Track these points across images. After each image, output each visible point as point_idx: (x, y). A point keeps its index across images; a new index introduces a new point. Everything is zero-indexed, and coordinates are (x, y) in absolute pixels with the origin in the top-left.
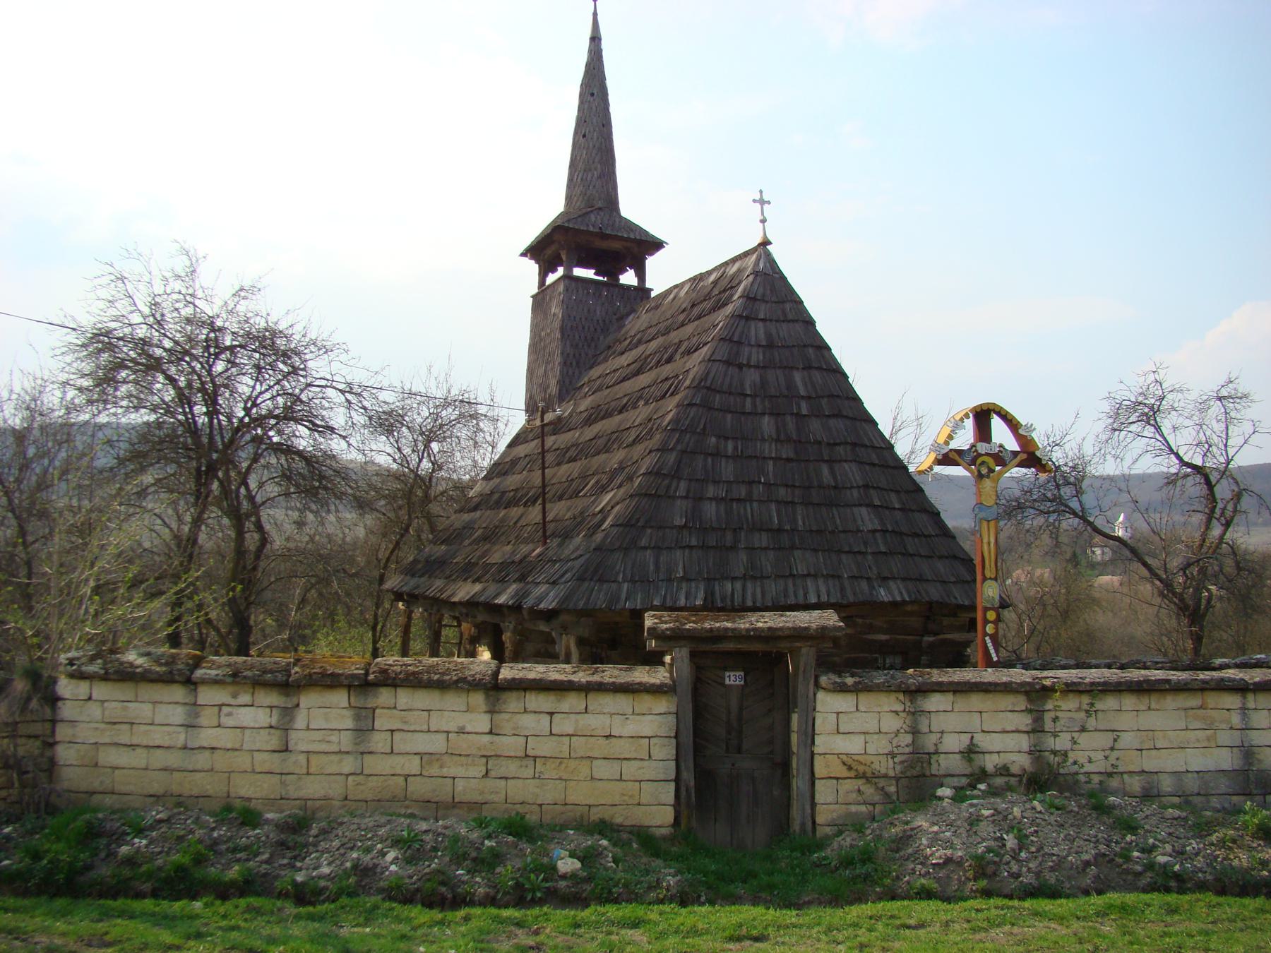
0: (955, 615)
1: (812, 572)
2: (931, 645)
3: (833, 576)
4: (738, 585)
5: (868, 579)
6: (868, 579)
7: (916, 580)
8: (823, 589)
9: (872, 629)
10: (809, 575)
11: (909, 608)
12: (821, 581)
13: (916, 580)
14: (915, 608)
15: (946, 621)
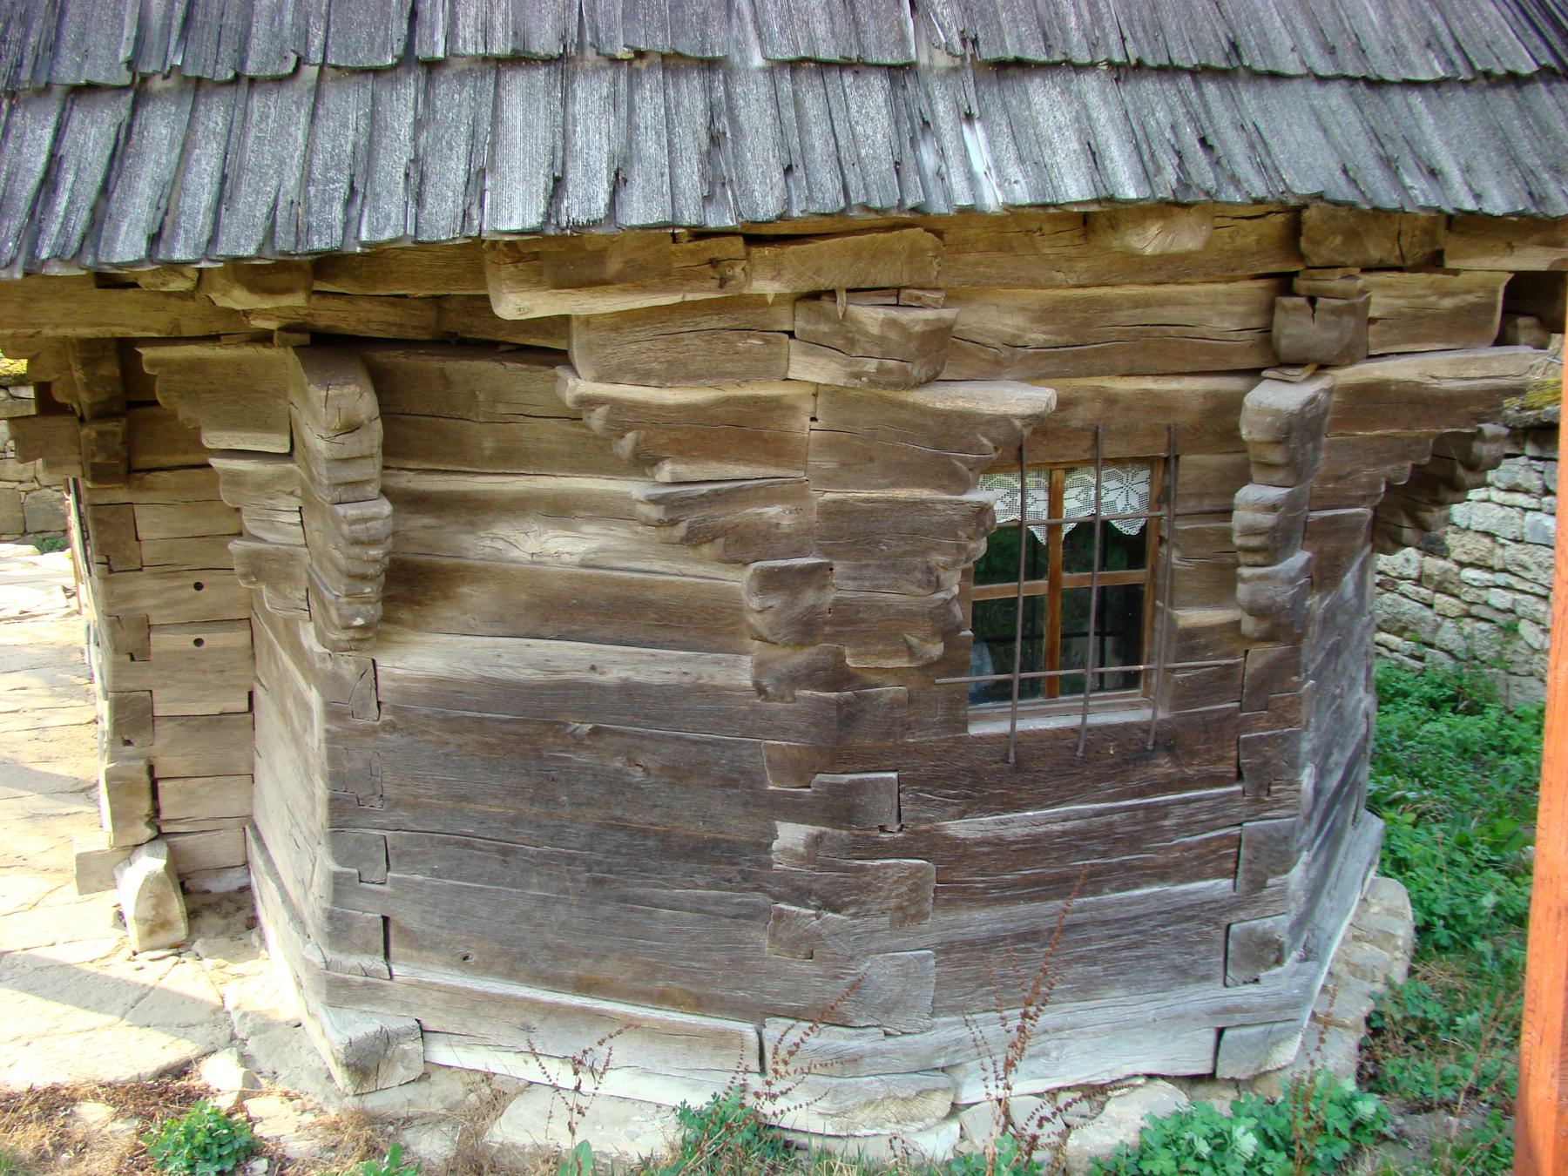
0: (1434, 262)
1: (544, 42)
2: (1298, 431)
3: (673, 63)
4: (93, 134)
5: (900, 73)
6: (900, 73)
7: (1201, 73)
8: (595, 142)
9: (942, 351)
10: (520, 59)
11: (1150, 240)
12: (590, 94)
13: (1201, 73)
14: (1188, 238)
15: (1386, 295)
